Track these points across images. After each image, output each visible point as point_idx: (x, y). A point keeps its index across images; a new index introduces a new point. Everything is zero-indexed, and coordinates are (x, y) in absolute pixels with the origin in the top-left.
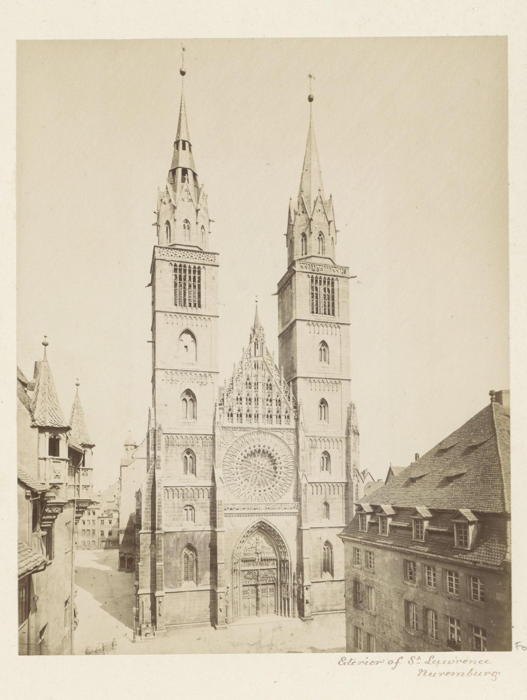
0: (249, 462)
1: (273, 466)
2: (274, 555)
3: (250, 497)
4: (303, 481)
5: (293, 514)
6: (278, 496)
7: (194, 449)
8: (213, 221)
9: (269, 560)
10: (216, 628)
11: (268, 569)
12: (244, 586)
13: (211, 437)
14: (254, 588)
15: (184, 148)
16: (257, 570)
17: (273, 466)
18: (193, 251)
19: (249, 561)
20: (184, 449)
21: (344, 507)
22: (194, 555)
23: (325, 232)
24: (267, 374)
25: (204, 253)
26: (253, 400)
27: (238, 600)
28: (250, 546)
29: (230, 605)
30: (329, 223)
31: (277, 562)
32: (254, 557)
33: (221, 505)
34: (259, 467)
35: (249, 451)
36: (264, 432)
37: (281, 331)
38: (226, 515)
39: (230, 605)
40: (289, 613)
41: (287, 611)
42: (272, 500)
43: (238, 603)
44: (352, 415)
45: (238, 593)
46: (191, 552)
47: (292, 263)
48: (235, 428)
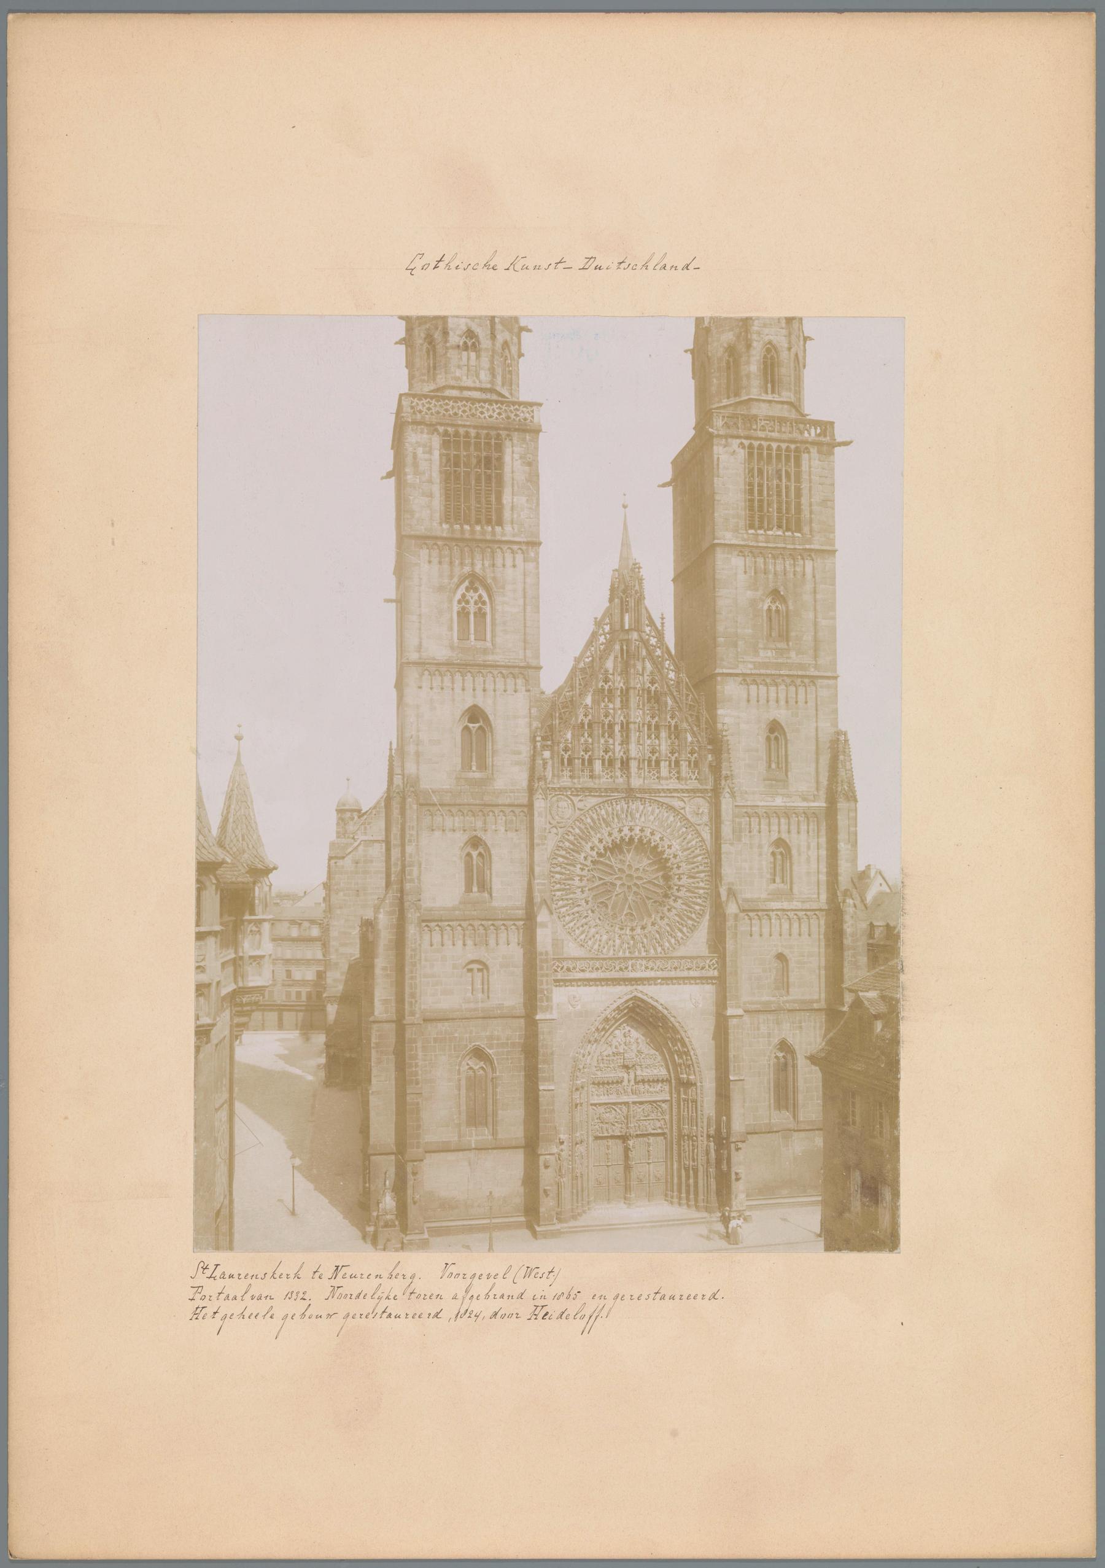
0: (607, 865)
1: (661, 873)
2: (663, 1072)
4: (732, 909)
5: (703, 980)
6: (673, 941)
7: (487, 838)
8: (529, 331)
9: (653, 1081)
10: (535, 1234)
11: (650, 1102)
12: (597, 1138)
13: (526, 810)
14: (619, 1142)
16: (626, 1104)
17: (661, 873)
19: (608, 1083)
20: (465, 837)
21: (823, 964)
22: (489, 1070)
23: (781, 341)
24: (649, 666)
26: (617, 728)
28: (609, 1051)
31: (671, 1085)
32: (620, 1075)
33: (546, 961)
34: (630, 876)
35: (609, 840)
36: (641, 798)
40: (696, 1200)
41: (692, 1196)
42: (659, 949)
43: (585, 1178)
44: (841, 757)
46: (482, 1064)
47: (704, 416)
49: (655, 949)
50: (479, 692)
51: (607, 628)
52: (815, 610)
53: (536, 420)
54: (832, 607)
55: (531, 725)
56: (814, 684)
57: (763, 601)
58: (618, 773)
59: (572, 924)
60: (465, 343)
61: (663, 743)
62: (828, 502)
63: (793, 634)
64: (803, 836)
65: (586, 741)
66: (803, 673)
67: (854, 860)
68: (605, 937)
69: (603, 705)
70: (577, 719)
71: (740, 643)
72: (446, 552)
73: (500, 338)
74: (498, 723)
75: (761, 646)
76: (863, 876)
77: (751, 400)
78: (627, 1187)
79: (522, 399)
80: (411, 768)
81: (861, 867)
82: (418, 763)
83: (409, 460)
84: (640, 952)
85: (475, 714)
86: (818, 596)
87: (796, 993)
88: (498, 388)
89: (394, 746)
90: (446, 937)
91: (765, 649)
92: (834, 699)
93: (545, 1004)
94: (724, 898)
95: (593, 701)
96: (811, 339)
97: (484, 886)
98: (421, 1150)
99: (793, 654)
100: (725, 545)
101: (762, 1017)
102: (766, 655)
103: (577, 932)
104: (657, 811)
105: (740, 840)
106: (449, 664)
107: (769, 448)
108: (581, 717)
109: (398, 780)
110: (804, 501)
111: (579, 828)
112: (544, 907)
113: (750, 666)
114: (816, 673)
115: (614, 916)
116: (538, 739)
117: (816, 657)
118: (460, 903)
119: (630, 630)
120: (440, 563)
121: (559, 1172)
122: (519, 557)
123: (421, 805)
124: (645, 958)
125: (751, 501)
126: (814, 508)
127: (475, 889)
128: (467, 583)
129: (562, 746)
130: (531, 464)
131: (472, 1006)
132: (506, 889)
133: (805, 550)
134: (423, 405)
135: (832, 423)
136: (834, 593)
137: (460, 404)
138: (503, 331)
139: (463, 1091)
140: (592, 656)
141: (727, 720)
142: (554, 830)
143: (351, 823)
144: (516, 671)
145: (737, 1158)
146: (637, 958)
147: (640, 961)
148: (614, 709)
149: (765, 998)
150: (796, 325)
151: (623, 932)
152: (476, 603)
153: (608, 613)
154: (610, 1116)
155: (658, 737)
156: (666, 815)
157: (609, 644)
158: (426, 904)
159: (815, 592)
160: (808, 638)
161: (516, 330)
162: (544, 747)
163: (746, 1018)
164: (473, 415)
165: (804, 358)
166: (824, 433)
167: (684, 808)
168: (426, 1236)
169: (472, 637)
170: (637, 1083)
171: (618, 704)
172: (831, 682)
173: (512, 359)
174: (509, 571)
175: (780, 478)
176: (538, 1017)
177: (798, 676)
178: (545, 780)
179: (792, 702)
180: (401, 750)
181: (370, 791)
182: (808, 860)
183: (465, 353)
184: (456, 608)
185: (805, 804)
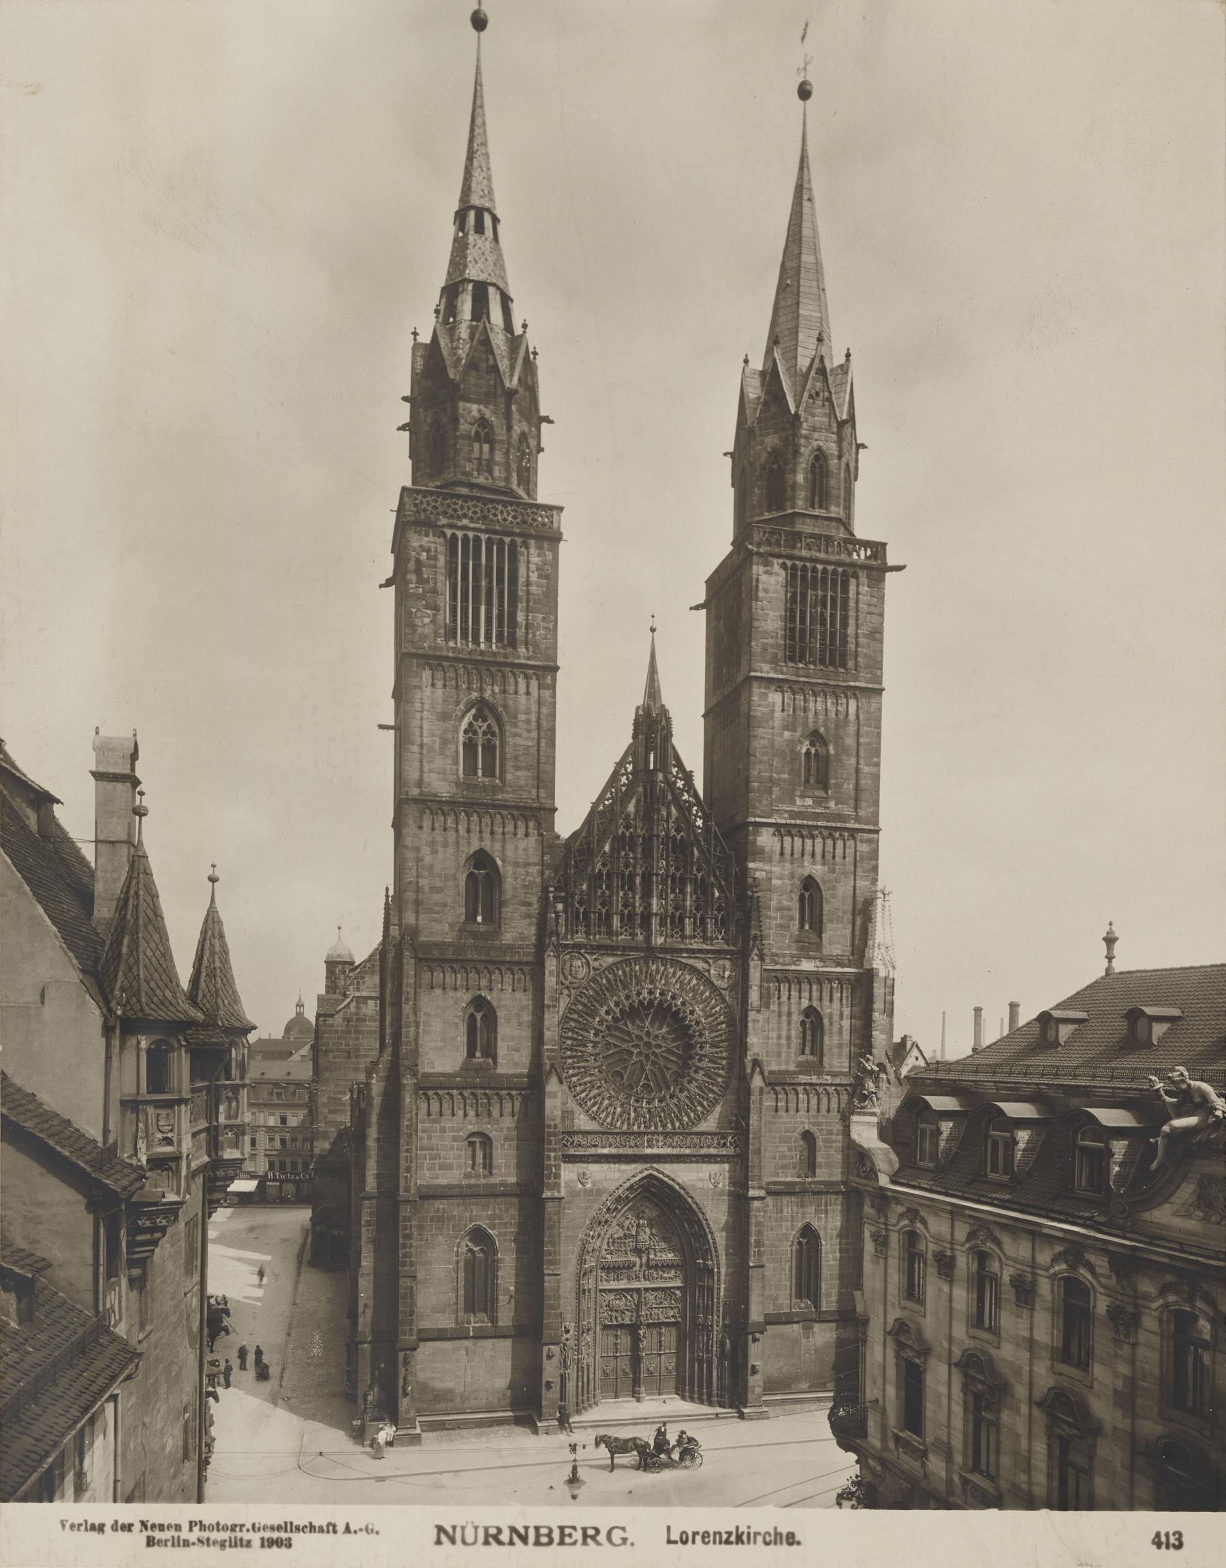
0: (623, 1031)
4: (757, 1082)
8: (551, 422)
11: (663, 1289)
12: (605, 1327)
15: (480, 229)
16: (638, 1290)
18: (498, 502)
19: (619, 1268)
20: (467, 997)
23: (832, 448)
26: (638, 880)
32: (632, 1259)
33: (555, 1135)
35: (627, 1004)
36: (662, 959)
37: (712, 704)
39: (572, 1372)
43: (591, 1370)
49: (673, 1125)
51: (630, 767)
53: (555, 525)
56: (854, 839)
57: (802, 743)
58: (638, 931)
59: (583, 1095)
60: (477, 432)
62: (876, 634)
64: (836, 1004)
66: (843, 825)
67: (890, 1033)
70: (593, 869)
72: (451, 674)
73: (517, 429)
74: (507, 871)
75: (798, 793)
76: (900, 1050)
80: (409, 918)
81: (897, 1039)
82: (417, 912)
83: (412, 566)
84: (656, 1128)
85: (481, 859)
86: (861, 740)
87: (822, 1175)
89: (391, 893)
90: (445, 1105)
91: (802, 796)
92: (874, 855)
93: (552, 1181)
94: (749, 1071)
95: (612, 849)
96: (863, 446)
97: (490, 1051)
99: (832, 804)
100: (762, 678)
101: (785, 1199)
102: (804, 803)
103: (589, 1104)
104: (679, 973)
105: (767, 1006)
107: (814, 570)
108: (598, 866)
110: (851, 630)
111: (594, 989)
113: (786, 816)
114: (857, 826)
115: (631, 1087)
116: (551, 889)
117: (856, 808)
118: (462, 1069)
119: (655, 769)
120: (445, 686)
121: (564, 1364)
122: (534, 683)
123: (420, 960)
125: (792, 630)
126: (861, 640)
127: (478, 1054)
128: (473, 711)
131: (473, 1181)
132: (512, 1057)
133: (850, 687)
135: (884, 545)
137: (470, 503)
138: (520, 421)
139: (462, 1275)
140: (612, 798)
141: (758, 875)
144: (527, 813)
145: (754, 1350)
146: (653, 1134)
148: (634, 858)
149: (789, 1179)
150: (847, 430)
152: (485, 733)
153: (631, 751)
154: (621, 1303)
155: (682, 892)
156: (688, 977)
157: (630, 785)
158: (425, 1068)
159: (858, 735)
160: (849, 786)
161: (535, 421)
164: (485, 518)
165: (857, 468)
166: (874, 556)
168: (418, 1431)
169: (480, 772)
170: (648, 1267)
175: (824, 606)
177: (836, 829)
178: (558, 935)
179: (829, 856)
181: (364, 941)
183: (476, 445)
185: (839, 970)
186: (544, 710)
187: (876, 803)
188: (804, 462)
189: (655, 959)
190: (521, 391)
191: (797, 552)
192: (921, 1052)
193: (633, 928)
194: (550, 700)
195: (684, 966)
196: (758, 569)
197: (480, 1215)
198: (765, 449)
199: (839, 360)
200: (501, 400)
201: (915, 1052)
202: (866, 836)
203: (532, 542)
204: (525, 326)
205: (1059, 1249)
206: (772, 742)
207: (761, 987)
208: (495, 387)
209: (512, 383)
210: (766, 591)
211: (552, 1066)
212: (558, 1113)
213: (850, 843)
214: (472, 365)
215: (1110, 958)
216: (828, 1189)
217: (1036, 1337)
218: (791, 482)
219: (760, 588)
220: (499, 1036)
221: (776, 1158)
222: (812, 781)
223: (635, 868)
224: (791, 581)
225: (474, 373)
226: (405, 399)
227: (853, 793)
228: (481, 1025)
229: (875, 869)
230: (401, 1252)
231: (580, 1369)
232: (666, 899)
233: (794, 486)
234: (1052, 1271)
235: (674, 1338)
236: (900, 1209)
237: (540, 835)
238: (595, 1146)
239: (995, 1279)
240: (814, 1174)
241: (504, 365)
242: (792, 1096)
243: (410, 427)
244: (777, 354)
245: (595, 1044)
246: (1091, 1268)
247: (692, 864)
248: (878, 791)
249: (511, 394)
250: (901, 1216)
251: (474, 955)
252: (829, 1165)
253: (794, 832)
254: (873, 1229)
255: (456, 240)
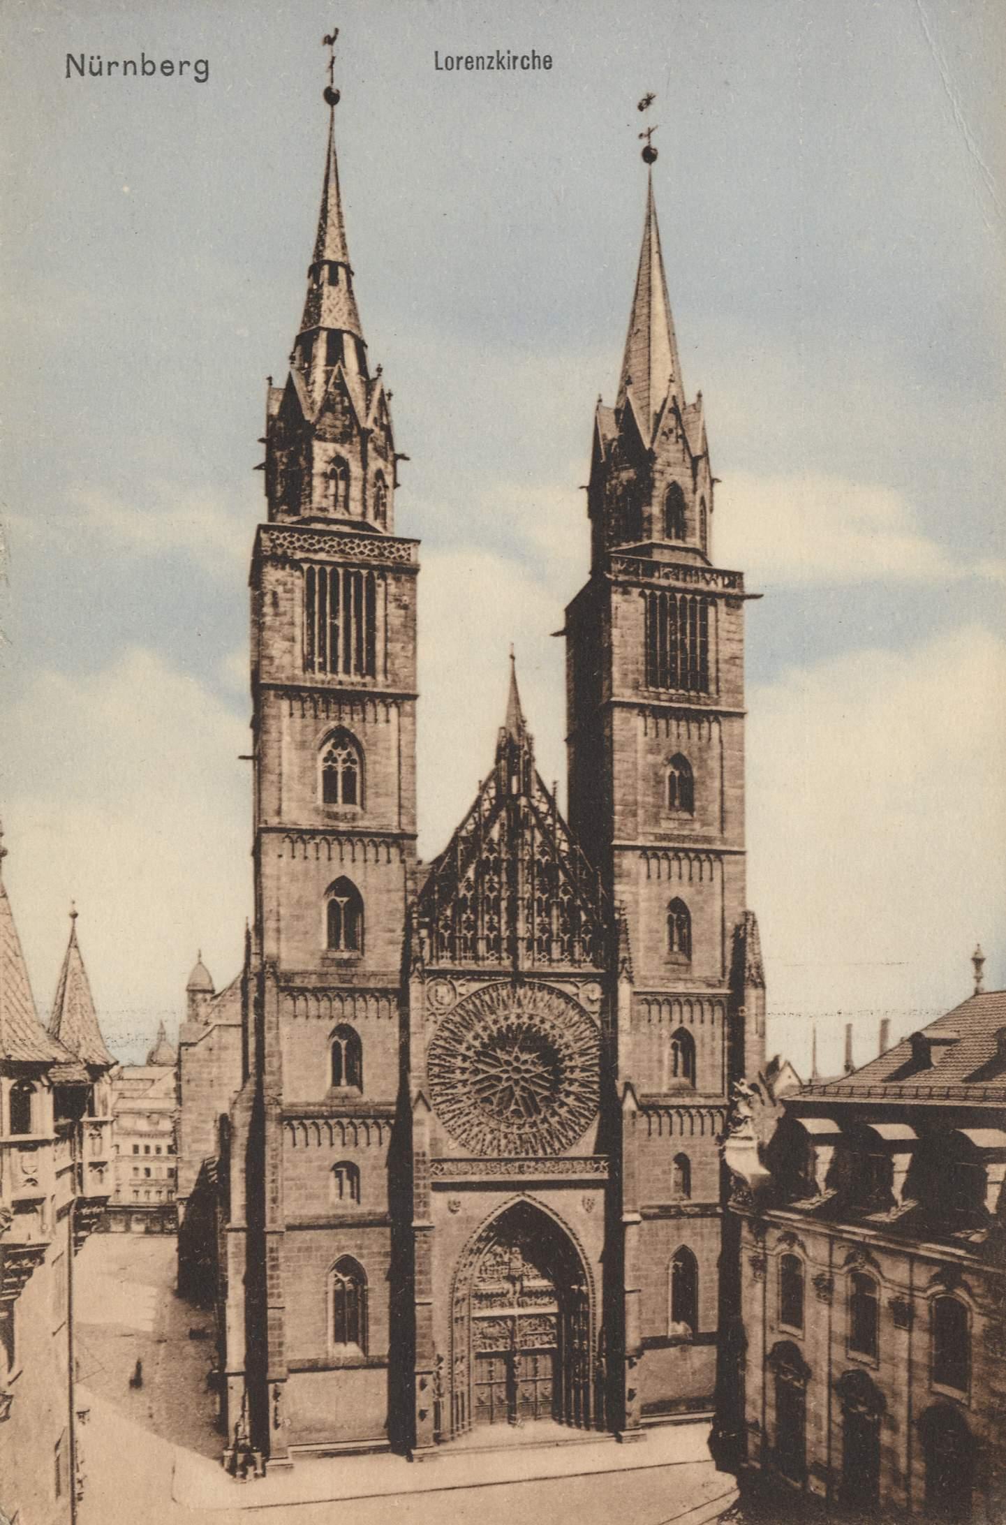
3: (495, 1143)
4: (629, 1104)
8: (407, 459)
12: (479, 1356)
15: (333, 281)
16: (512, 1318)
20: (333, 1024)
23: (686, 482)
25: (382, 539)
26: (504, 904)
27: (465, 1389)
29: (446, 1400)
30: (695, 461)
35: (494, 1028)
38: (438, 1187)
44: (749, 940)
45: (466, 1373)
47: (600, 561)
48: (459, 975)
50: (347, 862)
51: (493, 793)
52: (722, 778)
53: (413, 559)
54: (740, 775)
55: (406, 899)
56: (721, 860)
58: (504, 955)
59: (452, 1122)
61: (554, 920)
62: (734, 659)
63: (697, 804)
65: (468, 918)
67: (762, 1052)
68: (489, 1137)
69: (487, 877)
71: (640, 812)
75: (663, 815)
76: (773, 1068)
77: (653, 545)
78: (510, 1407)
79: (398, 535)
81: (769, 1058)
83: (268, 599)
84: (527, 1153)
85: (343, 886)
86: (725, 763)
87: (698, 1197)
88: (370, 519)
93: (421, 1209)
94: (620, 1094)
96: (718, 481)
97: (356, 1080)
98: (285, 1370)
99: (697, 826)
106: (313, 833)
109: (255, 961)
110: (711, 656)
112: (420, 1102)
113: (652, 838)
115: (500, 1113)
117: (722, 830)
120: (303, 716)
122: (393, 711)
124: (531, 1159)
126: (722, 666)
127: (343, 1082)
128: (332, 741)
129: (441, 923)
130: (409, 610)
132: (379, 1084)
133: (711, 712)
134: (285, 538)
135: (740, 575)
136: (742, 759)
141: (624, 897)
142: (432, 1018)
143: (204, 1005)
147: (527, 1163)
150: (702, 464)
151: (509, 1130)
152: (344, 761)
153: (495, 775)
154: (494, 1331)
155: (549, 915)
157: (495, 811)
158: (287, 1099)
159: (722, 758)
160: (715, 808)
161: (391, 458)
162: (422, 925)
163: (645, 1224)
164: (342, 551)
165: (712, 502)
167: (577, 995)
169: (340, 799)
171: (504, 879)
172: (738, 857)
173: (386, 487)
174: (382, 725)
176: (414, 1224)
179: (696, 879)
180: (259, 928)
182: (713, 1053)
184: (320, 766)
186: (404, 738)
187: (742, 824)
188: (660, 490)
189: (523, 984)
190: (377, 430)
191: (654, 580)
192: (793, 1071)
193: (499, 951)
194: (410, 727)
195: (551, 991)
196: (616, 598)
197: (347, 1243)
198: (621, 484)
199: (691, 399)
200: (356, 440)
201: (788, 1071)
202: (733, 858)
203: (390, 576)
204: (379, 370)
205: (936, 1269)
206: (635, 764)
207: (631, 1010)
208: (351, 426)
209: (368, 424)
210: (625, 618)
211: (420, 1095)
212: (427, 1140)
213: (717, 865)
214: (328, 405)
215: (978, 979)
216: (705, 1211)
217: (914, 1358)
218: (646, 515)
219: (619, 615)
220: (364, 1063)
221: (650, 1180)
222: (677, 803)
223: (499, 892)
224: (650, 611)
225: (329, 414)
226: (262, 440)
227: (717, 814)
228: (347, 1056)
229: (743, 889)
230: (269, 1283)
231: (454, 1397)
232: (532, 923)
233: (650, 519)
234: (929, 1292)
235: (550, 1365)
236: (777, 1233)
237: (403, 861)
238: (466, 1173)
239: (873, 1303)
240: (689, 1198)
241: (359, 406)
242: (665, 1119)
243: (268, 467)
244: (630, 394)
245: (463, 1070)
246: (969, 1289)
247: (558, 887)
248: (743, 812)
249: (365, 435)
250: (780, 1240)
251: (340, 984)
252: (705, 1187)
253: (660, 854)
254: (751, 1254)
255: (310, 291)
